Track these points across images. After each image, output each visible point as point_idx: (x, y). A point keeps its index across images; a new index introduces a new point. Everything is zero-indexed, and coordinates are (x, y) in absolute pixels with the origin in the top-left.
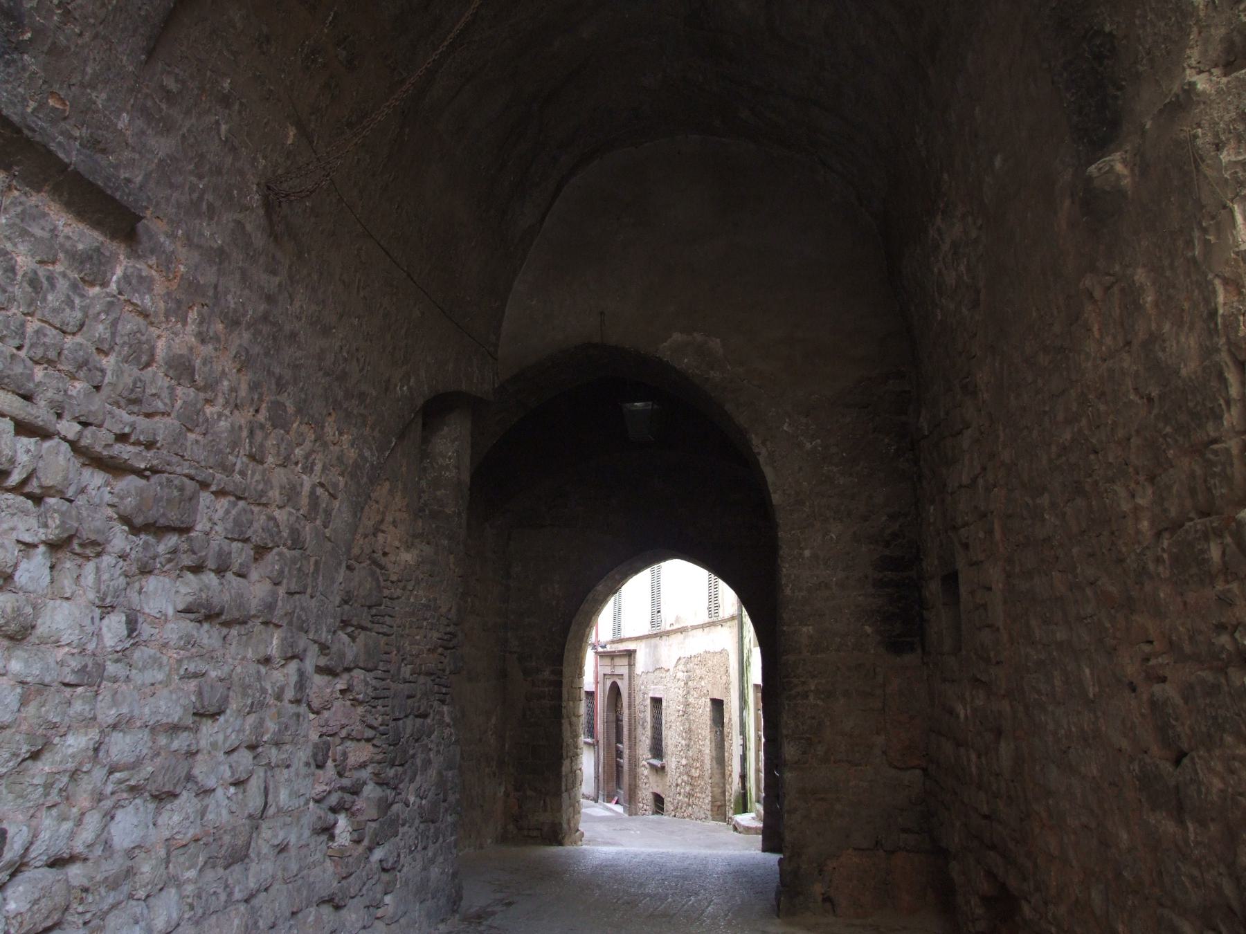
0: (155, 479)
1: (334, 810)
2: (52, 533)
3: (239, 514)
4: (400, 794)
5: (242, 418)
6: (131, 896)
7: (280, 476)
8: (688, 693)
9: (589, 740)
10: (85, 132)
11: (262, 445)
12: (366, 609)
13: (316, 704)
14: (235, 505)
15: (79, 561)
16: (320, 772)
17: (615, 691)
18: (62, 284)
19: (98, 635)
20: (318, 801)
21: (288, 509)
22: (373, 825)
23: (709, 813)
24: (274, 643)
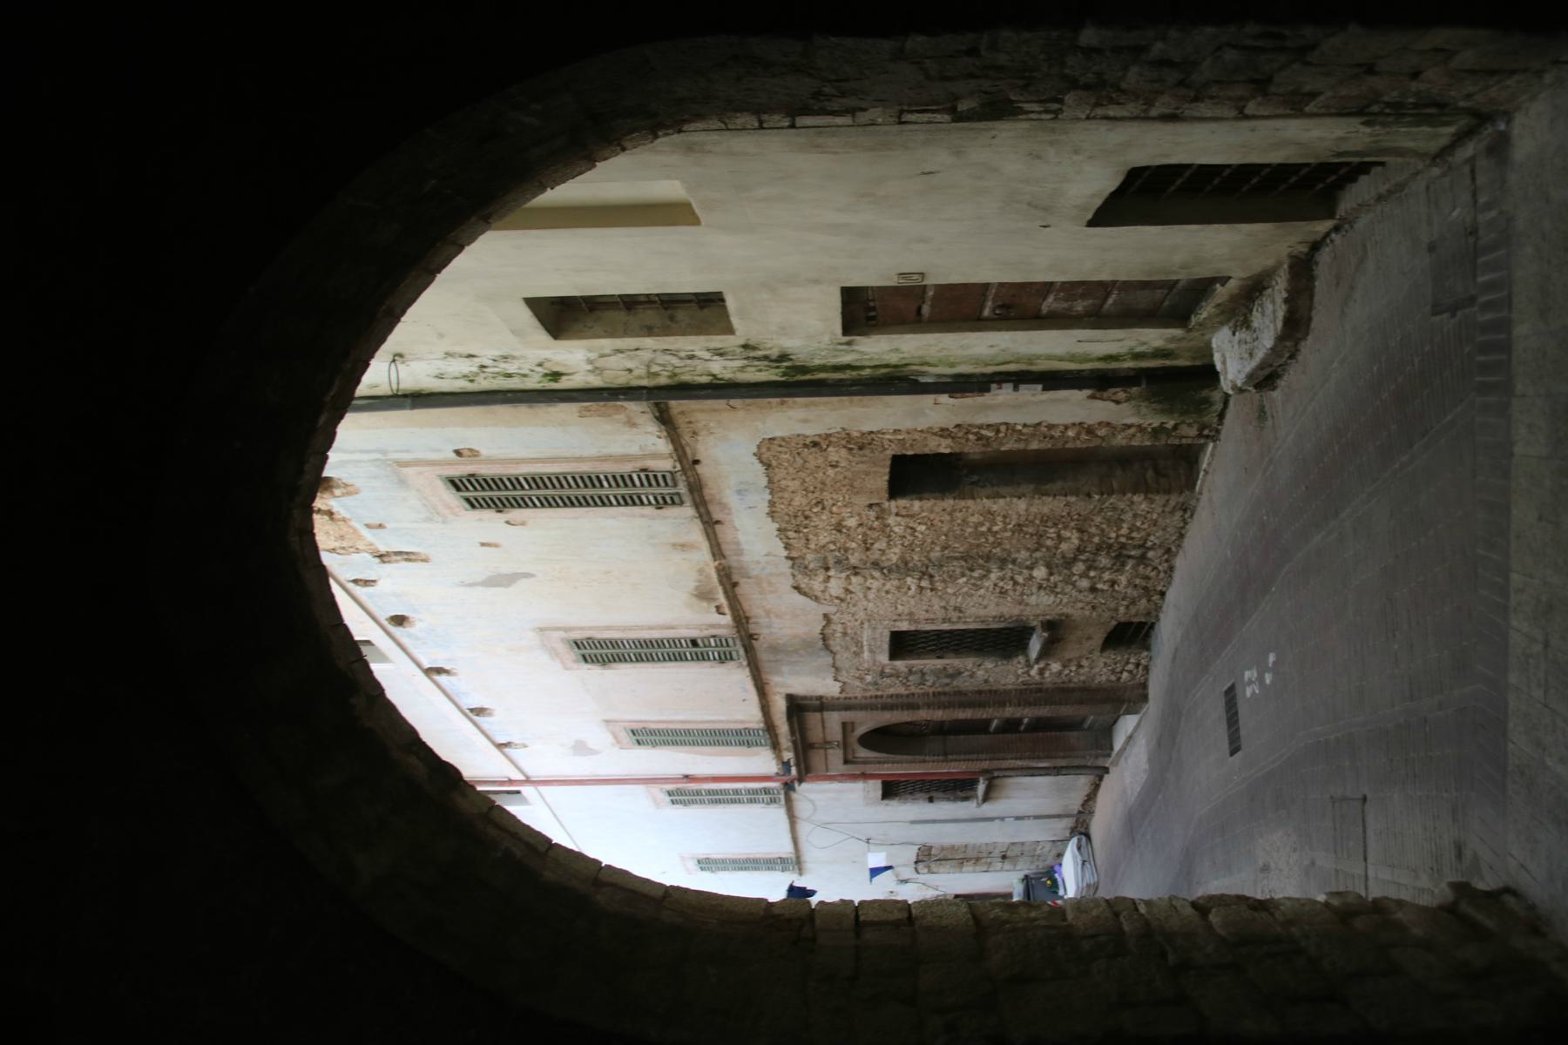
8: (876, 565)
9: (981, 788)
17: (881, 739)
23: (1174, 499)
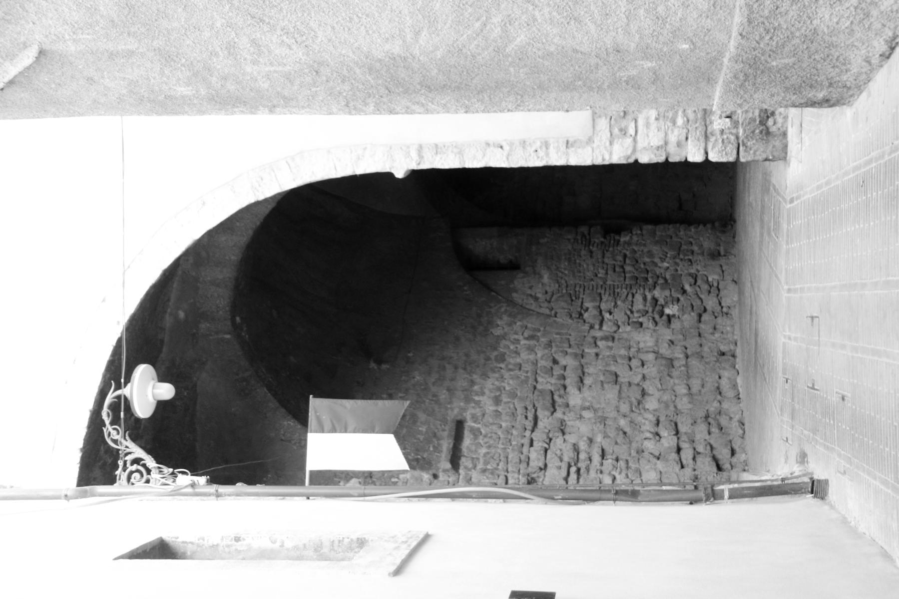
0: (536, 405)
1: (662, 314)
2: (560, 434)
3: (543, 373)
4: (661, 274)
5: (507, 375)
6: (674, 402)
7: (524, 355)
10: (434, 440)
11: (515, 365)
12: (573, 303)
13: (615, 328)
14: (539, 374)
15: (567, 426)
16: (644, 325)
18: (486, 440)
19: (589, 419)
20: (656, 323)
21: (536, 350)
22: (673, 290)
24: (590, 351)
